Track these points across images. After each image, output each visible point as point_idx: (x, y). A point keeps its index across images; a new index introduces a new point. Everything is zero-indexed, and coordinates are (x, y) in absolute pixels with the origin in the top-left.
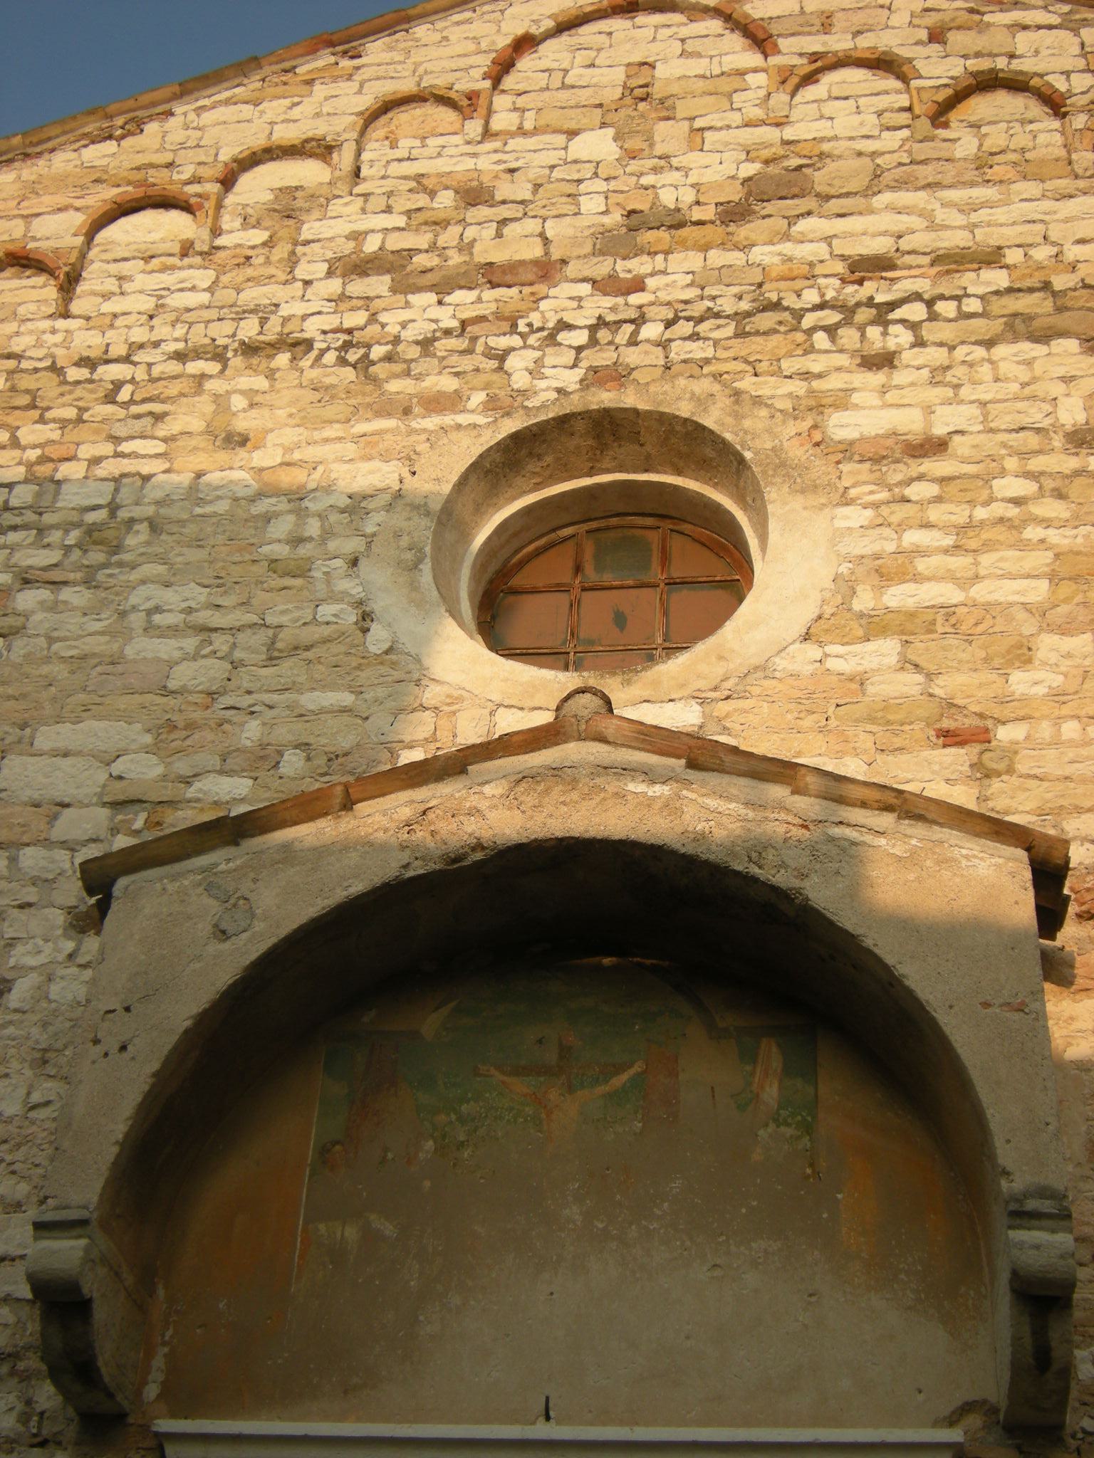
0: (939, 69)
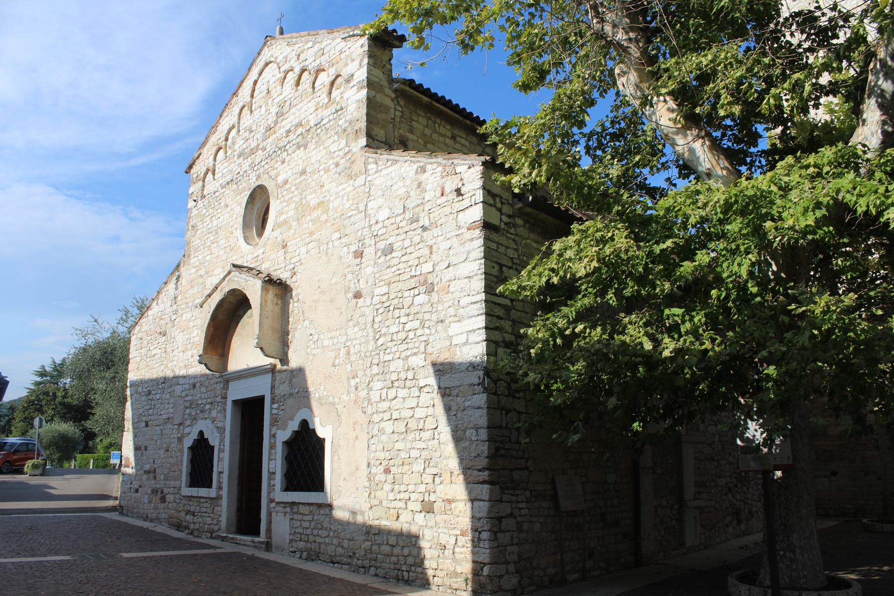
0: (297, 70)
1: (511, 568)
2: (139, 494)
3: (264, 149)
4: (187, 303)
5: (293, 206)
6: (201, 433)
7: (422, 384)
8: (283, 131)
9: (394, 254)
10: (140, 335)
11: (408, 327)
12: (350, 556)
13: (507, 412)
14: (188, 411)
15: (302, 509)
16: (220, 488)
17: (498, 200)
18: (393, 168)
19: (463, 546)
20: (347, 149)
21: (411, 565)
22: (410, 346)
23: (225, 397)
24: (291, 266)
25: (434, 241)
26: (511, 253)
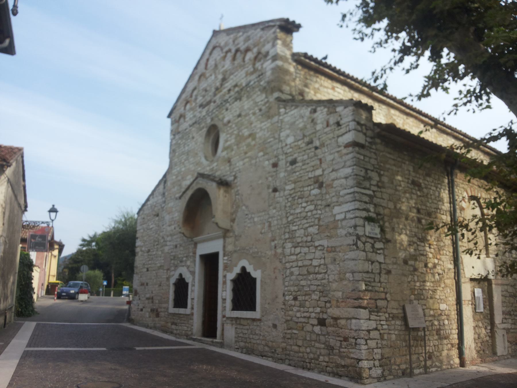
0: (233, 51)
1: (377, 363)
2: (143, 312)
3: (215, 102)
4: (171, 197)
5: (234, 136)
6: (181, 275)
7: (317, 244)
8: (225, 90)
9: (297, 165)
10: (143, 216)
11: (307, 210)
12: (273, 352)
13: (373, 263)
14: (172, 261)
15: (242, 322)
16: (192, 308)
17: (364, 127)
18: (296, 111)
19: (346, 348)
20: (266, 100)
21: (312, 359)
22: (309, 220)
23: (195, 253)
24: (234, 174)
25: (322, 155)
26: (373, 161)
